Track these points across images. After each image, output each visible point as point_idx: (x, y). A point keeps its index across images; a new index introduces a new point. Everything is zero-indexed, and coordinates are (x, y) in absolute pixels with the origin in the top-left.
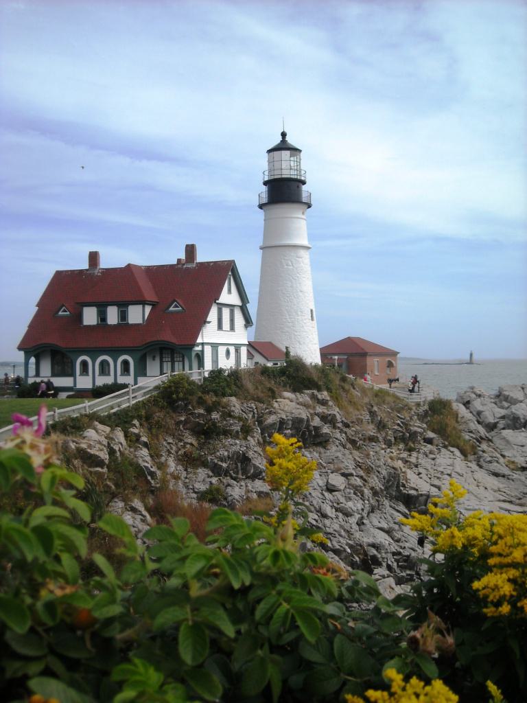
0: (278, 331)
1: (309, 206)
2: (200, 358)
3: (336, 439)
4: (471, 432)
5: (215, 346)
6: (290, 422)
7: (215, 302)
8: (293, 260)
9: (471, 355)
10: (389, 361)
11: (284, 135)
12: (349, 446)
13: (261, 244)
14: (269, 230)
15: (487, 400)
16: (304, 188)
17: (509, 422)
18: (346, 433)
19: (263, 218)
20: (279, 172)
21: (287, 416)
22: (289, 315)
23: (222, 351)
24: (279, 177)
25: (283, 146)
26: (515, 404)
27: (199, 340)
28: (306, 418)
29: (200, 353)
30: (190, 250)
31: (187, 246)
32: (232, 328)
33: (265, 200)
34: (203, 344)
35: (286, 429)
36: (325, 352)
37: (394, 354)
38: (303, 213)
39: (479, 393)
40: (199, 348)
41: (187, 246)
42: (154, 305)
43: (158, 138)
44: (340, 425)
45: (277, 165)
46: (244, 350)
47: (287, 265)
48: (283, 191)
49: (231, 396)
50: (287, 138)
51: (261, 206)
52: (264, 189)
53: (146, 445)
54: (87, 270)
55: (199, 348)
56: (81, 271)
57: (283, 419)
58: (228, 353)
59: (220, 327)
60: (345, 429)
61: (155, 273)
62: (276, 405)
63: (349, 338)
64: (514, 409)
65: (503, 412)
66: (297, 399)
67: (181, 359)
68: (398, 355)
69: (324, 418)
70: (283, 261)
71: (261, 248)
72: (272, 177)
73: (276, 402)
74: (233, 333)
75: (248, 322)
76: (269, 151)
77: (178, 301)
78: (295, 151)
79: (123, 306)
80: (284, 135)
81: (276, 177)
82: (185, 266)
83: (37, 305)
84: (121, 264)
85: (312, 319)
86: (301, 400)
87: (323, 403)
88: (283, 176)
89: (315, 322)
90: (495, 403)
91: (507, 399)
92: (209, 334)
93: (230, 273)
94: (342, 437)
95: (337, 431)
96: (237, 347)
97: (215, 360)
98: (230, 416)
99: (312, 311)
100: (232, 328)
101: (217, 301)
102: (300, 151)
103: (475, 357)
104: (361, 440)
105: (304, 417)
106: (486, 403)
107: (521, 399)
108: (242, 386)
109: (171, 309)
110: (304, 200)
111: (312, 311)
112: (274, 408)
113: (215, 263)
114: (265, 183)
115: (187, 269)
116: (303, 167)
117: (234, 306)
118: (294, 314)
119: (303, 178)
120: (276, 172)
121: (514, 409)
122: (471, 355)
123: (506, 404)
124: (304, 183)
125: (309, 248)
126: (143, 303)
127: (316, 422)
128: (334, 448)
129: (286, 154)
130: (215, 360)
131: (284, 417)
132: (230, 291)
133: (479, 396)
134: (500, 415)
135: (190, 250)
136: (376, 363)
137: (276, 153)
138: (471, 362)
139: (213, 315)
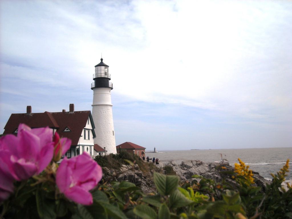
0: (100, 140)
1: (112, 89)
2: (78, 151)
3: (143, 183)
4: (182, 179)
5: (83, 146)
6: (128, 177)
8: (106, 111)
9: (155, 149)
10: (142, 152)
11: (102, 60)
12: (147, 186)
13: (92, 103)
14: (95, 98)
15: (178, 167)
16: (110, 81)
17: (188, 175)
18: (146, 181)
19: (93, 93)
20: (100, 75)
21: (127, 174)
22: (105, 133)
23: (85, 148)
24: (100, 77)
25: (101, 64)
26: (190, 168)
27: (78, 144)
29: (78, 149)
30: (72, 106)
31: (70, 105)
32: (89, 139)
33: (94, 86)
34: (79, 145)
35: (127, 180)
36: (118, 148)
37: (144, 149)
38: (110, 92)
39: (174, 164)
40: (78, 147)
41: (70, 105)
42: (57, 129)
43: (55, 59)
44: (143, 178)
45: (99, 72)
46: (93, 147)
47: (103, 113)
48: (101, 83)
49: (105, 166)
50: (104, 61)
51: (92, 89)
52: (94, 81)
54: (26, 114)
56: (23, 114)
57: (126, 176)
60: (145, 179)
61: (56, 115)
62: (121, 170)
63: (126, 143)
64: (190, 170)
65: (185, 171)
66: (128, 167)
67: (70, 152)
68: (146, 149)
69: (138, 174)
70: (102, 111)
71: (92, 106)
72: (97, 77)
73: (121, 169)
74: (88, 140)
75: (94, 136)
76: (96, 66)
77: (68, 127)
78: (106, 66)
80: (102, 60)
81: (99, 77)
82: (69, 113)
83: (4, 129)
84: (43, 112)
86: (129, 168)
88: (102, 77)
89: (114, 136)
90: (181, 168)
91: (186, 166)
92: (82, 141)
94: (145, 182)
95: (143, 180)
96: (91, 146)
98: (108, 175)
99: (113, 131)
100: (89, 139)
101: (84, 128)
102: (109, 66)
103: (156, 149)
104: (151, 183)
106: (177, 168)
107: (192, 166)
108: (108, 162)
109: (65, 130)
110: (110, 86)
111: (113, 131)
112: (121, 171)
113: (82, 112)
114: (94, 79)
115: (70, 114)
118: (106, 133)
119: (109, 77)
120: (99, 75)
121: (190, 170)
122: (155, 149)
123: (186, 168)
124: (110, 79)
125: (112, 106)
126: (53, 128)
127: (136, 177)
128: (144, 187)
129: (103, 68)
131: (126, 175)
133: (174, 165)
134: (184, 173)
135: (72, 106)
136: (138, 152)
137: (99, 67)
138: (155, 152)
139: (83, 134)
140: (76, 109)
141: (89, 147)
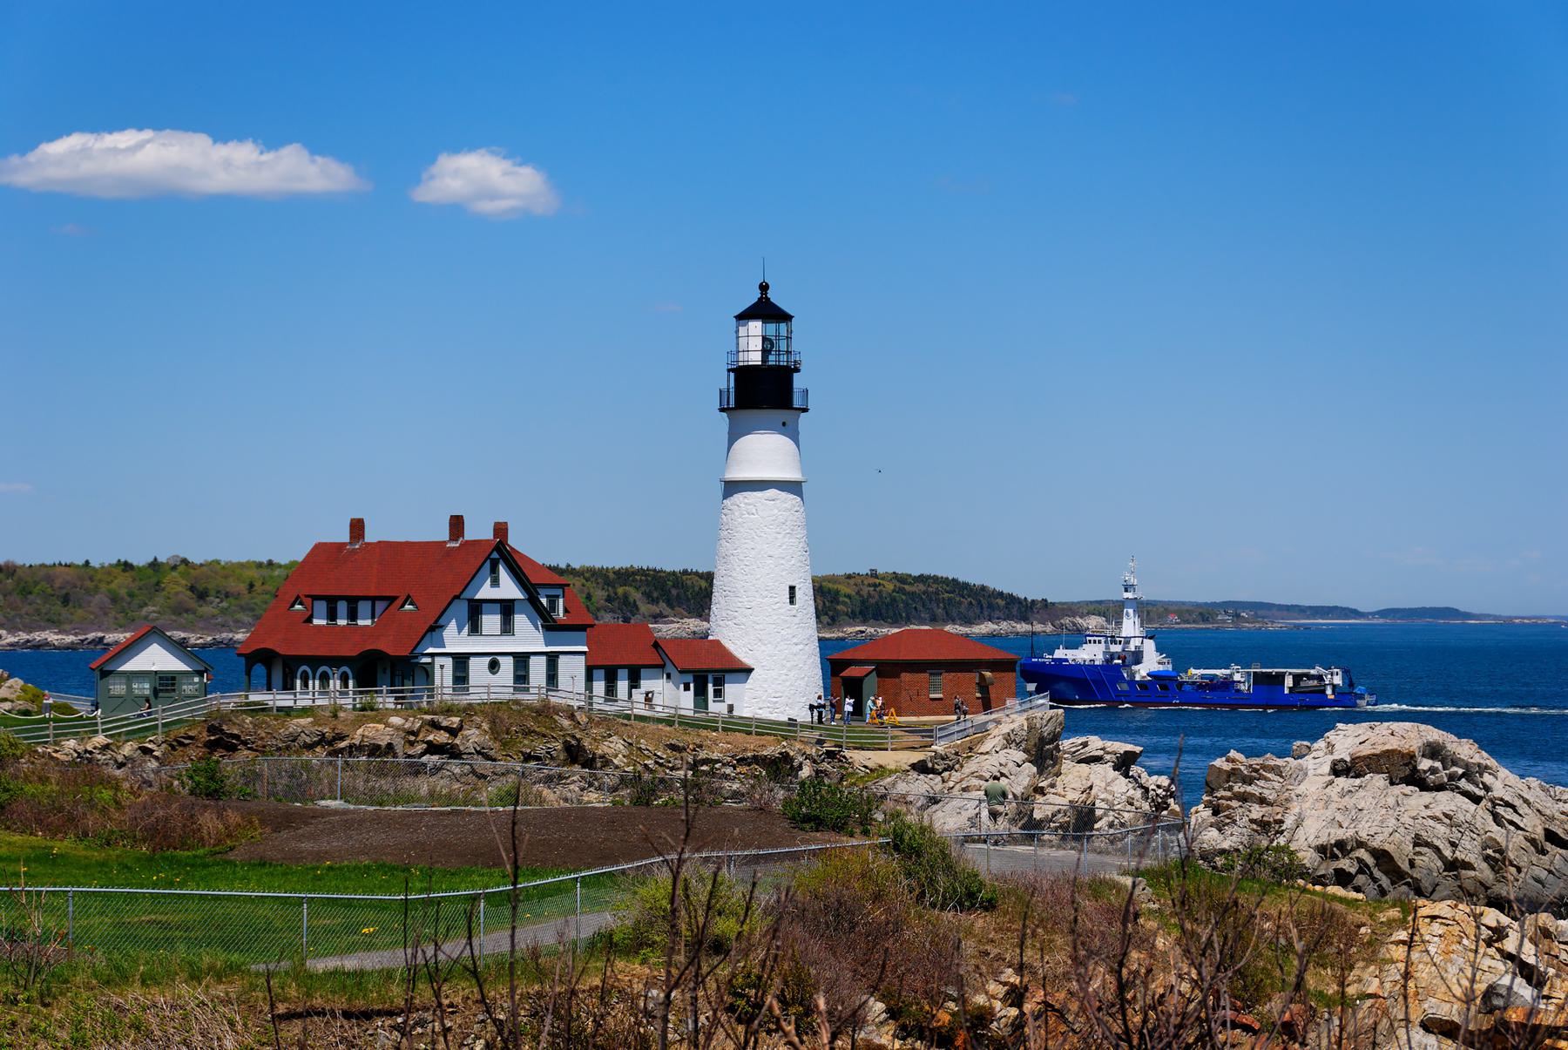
1: (805, 410)
2: (428, 673)
5: (461, 661)
7: (457, 597)
11: (764, 288)
25: (765, 310)
28: (383, 744)
33: (732, 404)
34: (432, 655)
50: (772, 295)
53: (157, 758)
55: (428, 660)
58: (494, 666)
59: (475, 629)
69: (433, 748)
79: (353, 602)
80: (764, 288)
85: (792, 601)
87: (453, 732)
93: (495, 555)
96: (522, 660)
97: (461, 677)
99: (792, 589)
105: (383, 744)
110: (797, 403)
111: (792, 589)
116: (794, 347)
117: (513, 601)
124: (797, 370)
129: (756, 327)
130: (461, 677)
132: (495, 583)
140: (470, 535)
141: (507, 664)
